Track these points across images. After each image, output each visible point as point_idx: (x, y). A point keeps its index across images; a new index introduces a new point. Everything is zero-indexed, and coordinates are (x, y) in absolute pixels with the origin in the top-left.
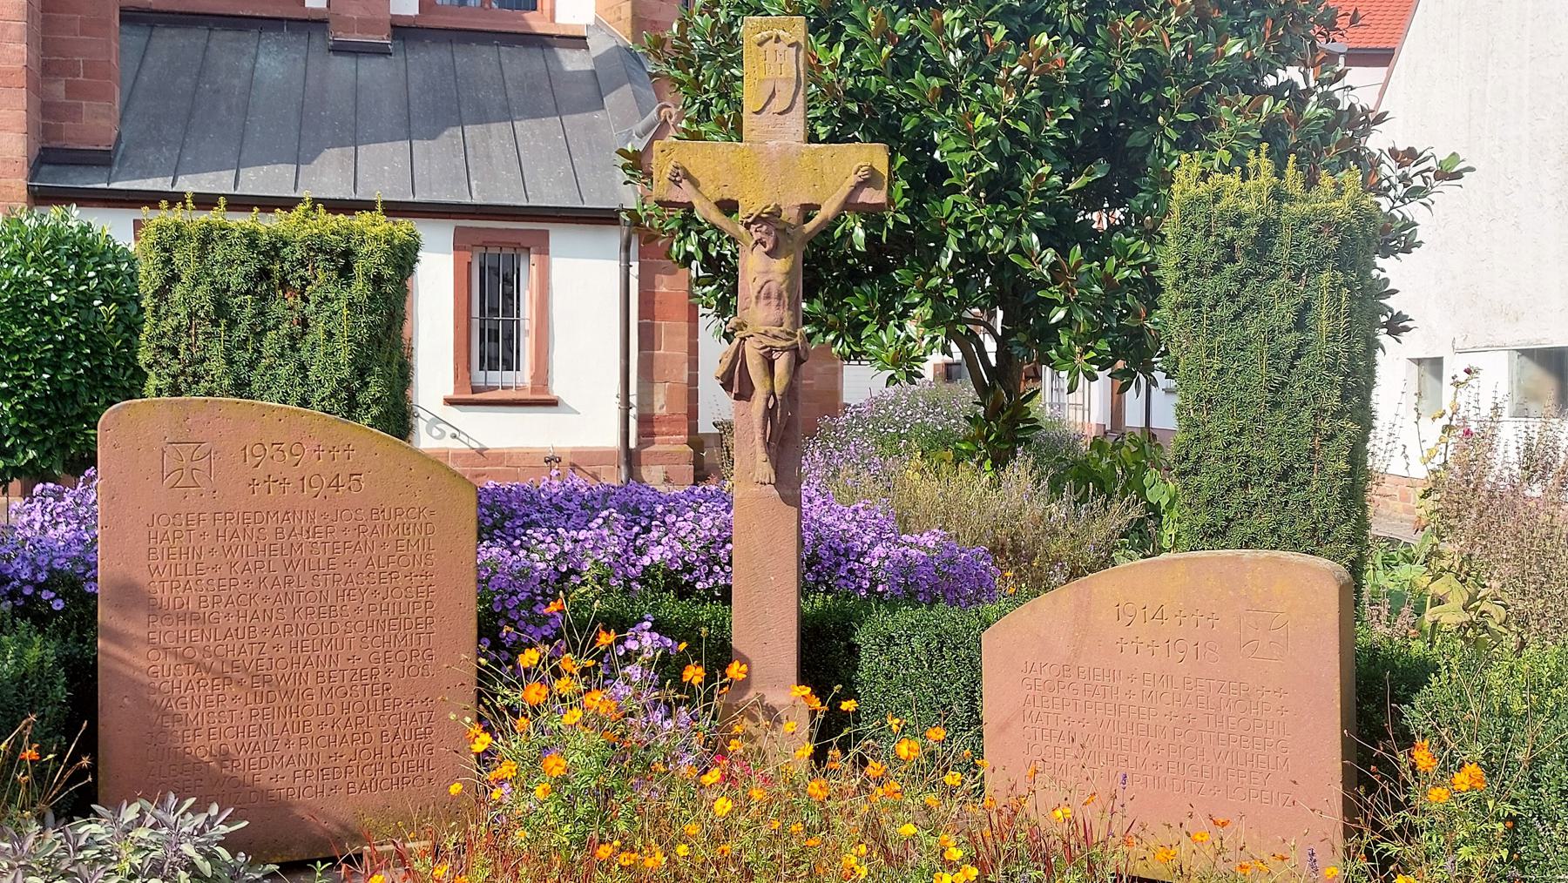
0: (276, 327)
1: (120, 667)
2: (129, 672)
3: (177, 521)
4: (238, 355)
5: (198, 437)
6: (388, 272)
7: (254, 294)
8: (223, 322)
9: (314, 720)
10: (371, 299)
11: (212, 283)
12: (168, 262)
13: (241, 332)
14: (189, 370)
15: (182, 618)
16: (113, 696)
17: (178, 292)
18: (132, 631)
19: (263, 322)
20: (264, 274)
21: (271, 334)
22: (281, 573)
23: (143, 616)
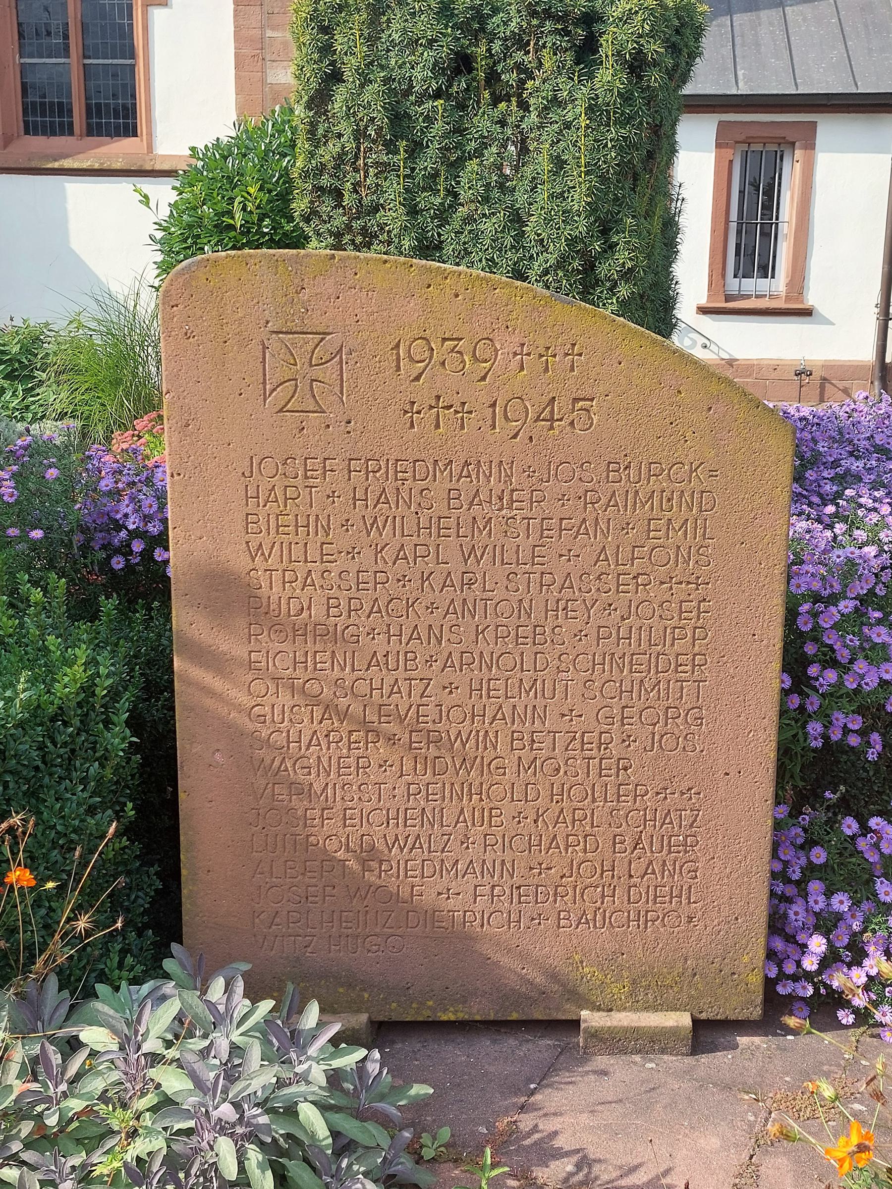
0: (478, 153)
1: (208, 702)
2: (223, 710)
3: (290, 470)
4: (423, 199)
5: (316, 321)
6: (654, 48)
7: (449, 97)
8: (402, 144)
9: (508, 809)
10: (626, 98)
11: (387, 80)
12: (326, 49)
13: (427, 162)
14: (357, 225)
15: (298, 632)
16: (197, 749)
17: (340, 95)
18: (224, 648)
19: (459, 146)
20: (463, 63)
21: (473, 165)
22: (456, 566)
23: (241, 622)
